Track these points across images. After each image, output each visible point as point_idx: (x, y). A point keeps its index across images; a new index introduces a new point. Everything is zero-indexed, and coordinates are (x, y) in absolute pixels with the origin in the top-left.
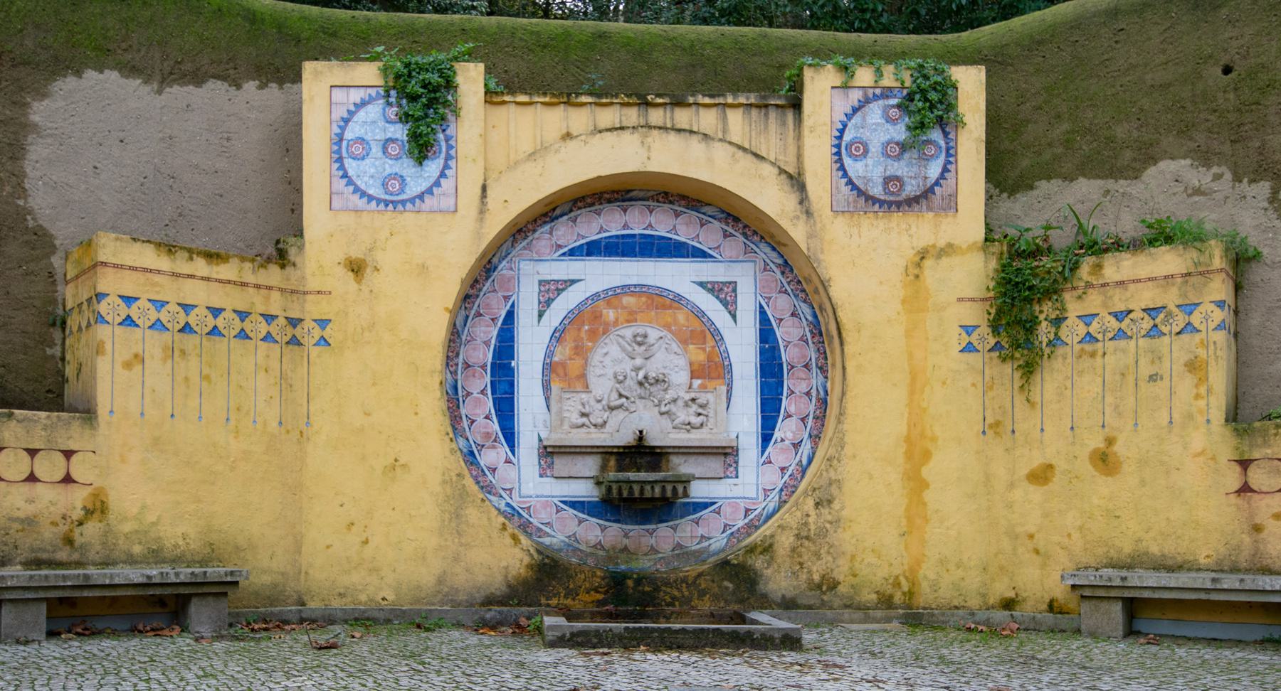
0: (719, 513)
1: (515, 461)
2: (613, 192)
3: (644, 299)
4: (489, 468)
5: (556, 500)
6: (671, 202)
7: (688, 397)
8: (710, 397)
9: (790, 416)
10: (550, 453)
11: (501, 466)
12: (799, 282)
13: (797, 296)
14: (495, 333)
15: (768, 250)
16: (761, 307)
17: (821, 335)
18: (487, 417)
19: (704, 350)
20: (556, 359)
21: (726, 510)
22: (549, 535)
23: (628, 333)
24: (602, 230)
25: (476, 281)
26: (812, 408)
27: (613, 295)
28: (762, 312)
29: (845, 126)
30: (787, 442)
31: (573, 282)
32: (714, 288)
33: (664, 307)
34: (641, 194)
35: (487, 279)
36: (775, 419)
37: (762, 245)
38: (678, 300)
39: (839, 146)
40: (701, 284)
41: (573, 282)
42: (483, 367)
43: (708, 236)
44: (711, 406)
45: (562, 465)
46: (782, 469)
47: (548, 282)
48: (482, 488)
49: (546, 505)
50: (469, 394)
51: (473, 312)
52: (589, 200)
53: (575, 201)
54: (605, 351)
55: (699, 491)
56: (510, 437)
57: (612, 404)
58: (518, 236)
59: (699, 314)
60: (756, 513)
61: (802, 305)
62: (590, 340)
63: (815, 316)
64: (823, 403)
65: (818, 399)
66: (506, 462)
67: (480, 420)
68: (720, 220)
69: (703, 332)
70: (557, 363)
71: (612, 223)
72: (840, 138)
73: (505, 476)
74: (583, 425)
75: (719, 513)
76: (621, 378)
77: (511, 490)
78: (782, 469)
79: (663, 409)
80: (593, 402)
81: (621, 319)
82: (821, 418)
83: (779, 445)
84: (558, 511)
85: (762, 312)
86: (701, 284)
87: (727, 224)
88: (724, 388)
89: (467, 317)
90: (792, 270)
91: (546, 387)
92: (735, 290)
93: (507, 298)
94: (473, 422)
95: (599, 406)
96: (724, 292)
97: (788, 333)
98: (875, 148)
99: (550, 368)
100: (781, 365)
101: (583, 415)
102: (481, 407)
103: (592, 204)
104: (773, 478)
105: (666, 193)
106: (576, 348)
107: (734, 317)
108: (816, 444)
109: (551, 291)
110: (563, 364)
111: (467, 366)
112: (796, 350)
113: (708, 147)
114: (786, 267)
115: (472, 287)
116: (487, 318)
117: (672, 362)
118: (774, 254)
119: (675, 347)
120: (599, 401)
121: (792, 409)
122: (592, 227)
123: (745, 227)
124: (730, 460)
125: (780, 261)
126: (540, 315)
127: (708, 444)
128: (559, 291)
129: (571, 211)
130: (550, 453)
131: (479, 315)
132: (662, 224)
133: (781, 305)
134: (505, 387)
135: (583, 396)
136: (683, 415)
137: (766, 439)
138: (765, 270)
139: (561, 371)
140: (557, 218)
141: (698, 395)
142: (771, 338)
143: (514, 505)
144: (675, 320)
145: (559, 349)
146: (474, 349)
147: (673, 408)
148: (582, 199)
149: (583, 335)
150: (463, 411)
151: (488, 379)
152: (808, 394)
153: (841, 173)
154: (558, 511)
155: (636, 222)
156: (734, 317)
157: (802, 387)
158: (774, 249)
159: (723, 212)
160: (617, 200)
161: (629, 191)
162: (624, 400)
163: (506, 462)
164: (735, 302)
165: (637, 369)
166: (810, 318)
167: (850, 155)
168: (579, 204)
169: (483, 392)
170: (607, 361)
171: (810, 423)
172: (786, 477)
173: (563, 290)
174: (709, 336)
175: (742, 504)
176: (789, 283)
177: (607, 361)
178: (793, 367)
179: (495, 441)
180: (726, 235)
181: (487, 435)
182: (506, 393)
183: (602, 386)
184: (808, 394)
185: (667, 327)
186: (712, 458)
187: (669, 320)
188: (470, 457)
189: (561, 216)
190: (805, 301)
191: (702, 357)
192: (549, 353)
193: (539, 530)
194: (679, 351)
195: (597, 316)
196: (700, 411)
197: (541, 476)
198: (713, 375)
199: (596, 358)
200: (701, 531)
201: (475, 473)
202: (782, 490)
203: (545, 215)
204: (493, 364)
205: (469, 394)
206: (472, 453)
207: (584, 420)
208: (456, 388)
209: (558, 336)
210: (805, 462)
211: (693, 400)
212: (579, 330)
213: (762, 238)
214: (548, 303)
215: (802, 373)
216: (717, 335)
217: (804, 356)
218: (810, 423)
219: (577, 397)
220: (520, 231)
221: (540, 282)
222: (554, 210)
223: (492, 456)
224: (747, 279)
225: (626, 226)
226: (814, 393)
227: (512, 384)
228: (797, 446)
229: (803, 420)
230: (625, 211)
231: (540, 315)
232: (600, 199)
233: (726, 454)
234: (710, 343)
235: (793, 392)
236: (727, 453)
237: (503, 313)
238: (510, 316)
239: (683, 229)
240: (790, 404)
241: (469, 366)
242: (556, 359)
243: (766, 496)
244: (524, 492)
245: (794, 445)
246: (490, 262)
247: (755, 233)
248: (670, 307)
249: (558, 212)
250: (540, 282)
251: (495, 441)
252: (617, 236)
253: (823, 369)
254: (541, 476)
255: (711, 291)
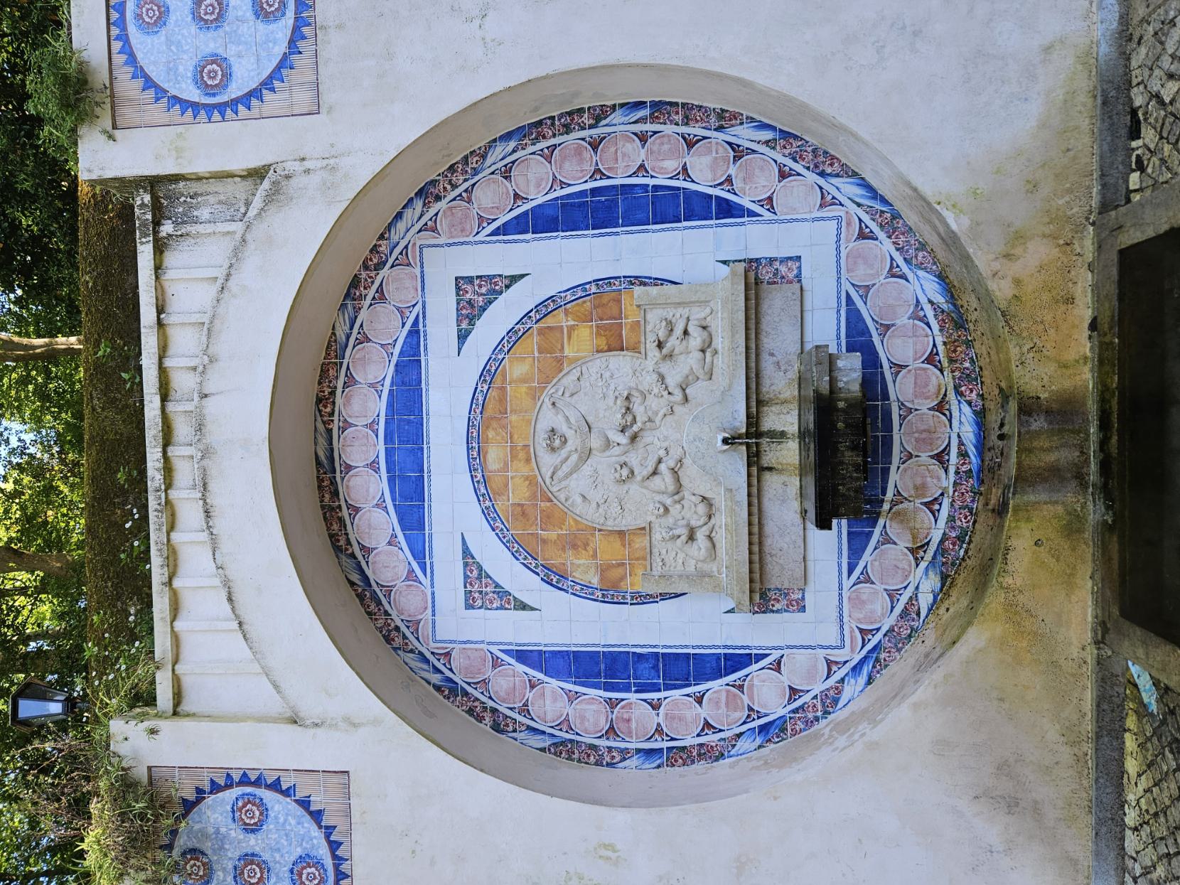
0: (868, 288)
1: (775, 655)
2: (320, 487)
3: (491, 434)
4: (790, 701)
5: (847, 584)
6: (333, 393)
7: (654, 353)
8: (654, 317)
9: (685, 169)
10: (762, 594)
11: (788, 677)
12: (452, 168)
13: (476, 172)
14: (554, 683)
15: (401, 226)
16: (496, 232)
17: (540, 123)
18: (699, 701)
19: (571, 329)
20: (595, 581)
21: (861, 275)
22: (914, 598)
23: (548, 461)
24: (381, 505)
25: (470, 712)
26: (669, 129)
27: (484, 488)
28: (504, 230)
29: (176, 100)
30: (732, 171)
31: (466, 552)
32: (469, 314)
33: (502, 399)
34: (322, 441)
35: (466, 694)
36: (689, 195)
37: (395, 237)
38: (487, 375)
39: (210, 108)
40: (463, 337)
41: (466, 552)
42: (612, 704)
43: (384, 326)
44: (669, 313)
45: (780, 574)
46: (783, 175)
47: (468, 594)
48: (826, 713)
49: (857, 602)
50: (659, 730)
51: (519, 718)
52: (335, 527)
53: (338, 549)
54: (579, 500)
55: (825, 329)
56: (734, 662)
57: (671, 488)
58: (398, 641)
59: (514, 336)
60: (866, 218)
61: (489, 161)
62: (562, 523)
63: (507, 137)
64: (660, 109)
65: (653, 119)
66: (778, 670)
67: (704, 712)
68: (357, 310)
69: (540, 332)
70: (602, 579)
71: (368, 488)
72: (195, 106)
73: (805, 672)
74: (710, 537)
75: (868, 288)
76: (625, 472)
77: (829, 663)
78: (783, 175)
79: (678, 396)
80: (670, 520)
81: (525, 471)
82: (689, 112)
83: (737, 184)
84: (869, 580)
85: (504, 230)
86: (463, 337)
87: (361, 298)
88: (638, 290)
89: (529, 728)
90: (433, 183)
91: (642, 599)
92: (470, 280)
93: (496, 662)
94: (707, 725)
95: (675, 510)
96: (475, 298)
97: (537, 183)
98: (210, 43)
99: (610, 593)
100: (594, 191)
101: (691, 538)
102: (681, 710)
103: (341, 521)
104: (800, 192)
105: (319, 401)
106: (574, 547)
107: (514, 279)
108: (735, 116)
109: (481, 590)
110: (603, 570)
111: (611, 731)
112: (567, 165)
113: (218, 330)
114: (427, 193)
115: (480, 719)
116: (530, 695)
117: (598, 383)
118: (408, 213)
119: (569, 380)
120: (667, 510)
121: (672, 165)
122: (376, 524)
123: (366, 267)
124: (766, 274)
125: (419, 204)
126: (524, 607)
127: (741, 316)
128: (482, 574)
129: (353, 556)
130: (762, 594)
131: (524, 710)
132: (366, 405)
133: (490, 196)
134: (644, 667)
135: (657, 536)
136: (689, 361)
137: (727, 210)
138: (434, 230)
139: (615, 574)
140: (366, 579)
141: (651, 338)
142: (549, 212)
143: (857, 658)
144: (523, 380)
145: (578, 576)
146: (583, 718)
147: (672, 381)
148: (333, 538)
149: (552, 535)
150: (690, 741)
151: (632, 697)
152: (643, 138)
153: (254, 102)
154: (869, 580)
155: (363, 450)
156: (514, 279)
157: (636, 153)
158: (399, 216)
159: (343, 306)
160: (333, 482)
161: (319, 463)
162: (663, 467)
163: (778, 670)
164: (490, 278)
165: (608, 444)
166: (512, 144)
167: (223, 85)
168: (342, 543)
169: (655, 706)
170: (595, 496)
171: (695, 130)
172: (798, 167)
173: (480, 568)
174: (549, 321)
175: (850, 245)
176: (454, 187)
177: (595, 496)
178: (598, 171)
179: (741, 688)
180: (381, 296)
181: (731, 703)
182: (656, 667)
183: (640, 504)
184: (643, 138)
185: (535, 395)
186: (765, 307)
187: (523, 388)
188: (770, 731)
189: (362, 572)
190: (484, 157)
191: (585, 333)
192: (585, 592)
193: (904, 614)
194: (576, 373)
195: (522, 512)
196: (679, 331)
197: (803, 609)
198: (615, 312)
199: (591, 515)
200: (903, 320)
201: (800, 725)
202: (822, 174)
203: (361, 597)
204: (609, 687)
205: (659, 730)
206: (764, 729)
207: (700, 535)
208: (650, 753)
209: (555, 577)
210: (767, 135)
211: (660, 345)
212: (544, 541)
213: (382, 237)
214: (502, 593)
215: (607, 149)
216: (547, 307)
217: (578, 152)
218: (695, 130)
219: (659, 547)
220: (388, 640)
221: (469, 606)
222: (352, 584)
223: (767, 693)
224: (448, 263)
225: (374, 466)
226: (638, 128)
227: (640, 657)
228: (738, 152)
229: (690, 144)
230: (349, 468)
231: (524, 607)
232: (332, 509)
233: (758, 282)
234: (560, 319)
235: (642, 166)
236: (756, 280)
237: (521, 668)
238: (522, 656)
239: (373, 370)
240: (663, 171)
241: (612, 728)
242: (595, 581)
243: (835, 202)
244: (833, 640)
245: (736, 159)
246: (438, 688)
247: (374, 249)
248: (503, 389)
249: (355, 577)
250: (469, 606)
251: (741, 688)
252: (391, 480)
253: (600, 114)
254: (803, 609)
255: (472, 320)
